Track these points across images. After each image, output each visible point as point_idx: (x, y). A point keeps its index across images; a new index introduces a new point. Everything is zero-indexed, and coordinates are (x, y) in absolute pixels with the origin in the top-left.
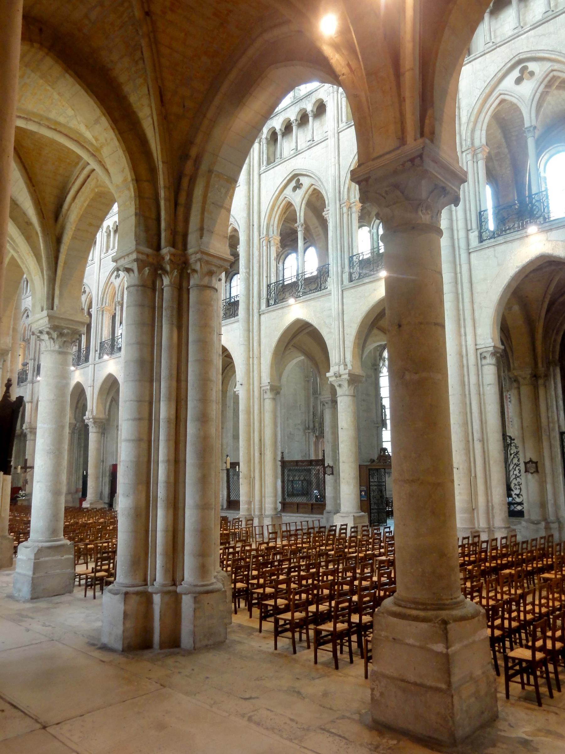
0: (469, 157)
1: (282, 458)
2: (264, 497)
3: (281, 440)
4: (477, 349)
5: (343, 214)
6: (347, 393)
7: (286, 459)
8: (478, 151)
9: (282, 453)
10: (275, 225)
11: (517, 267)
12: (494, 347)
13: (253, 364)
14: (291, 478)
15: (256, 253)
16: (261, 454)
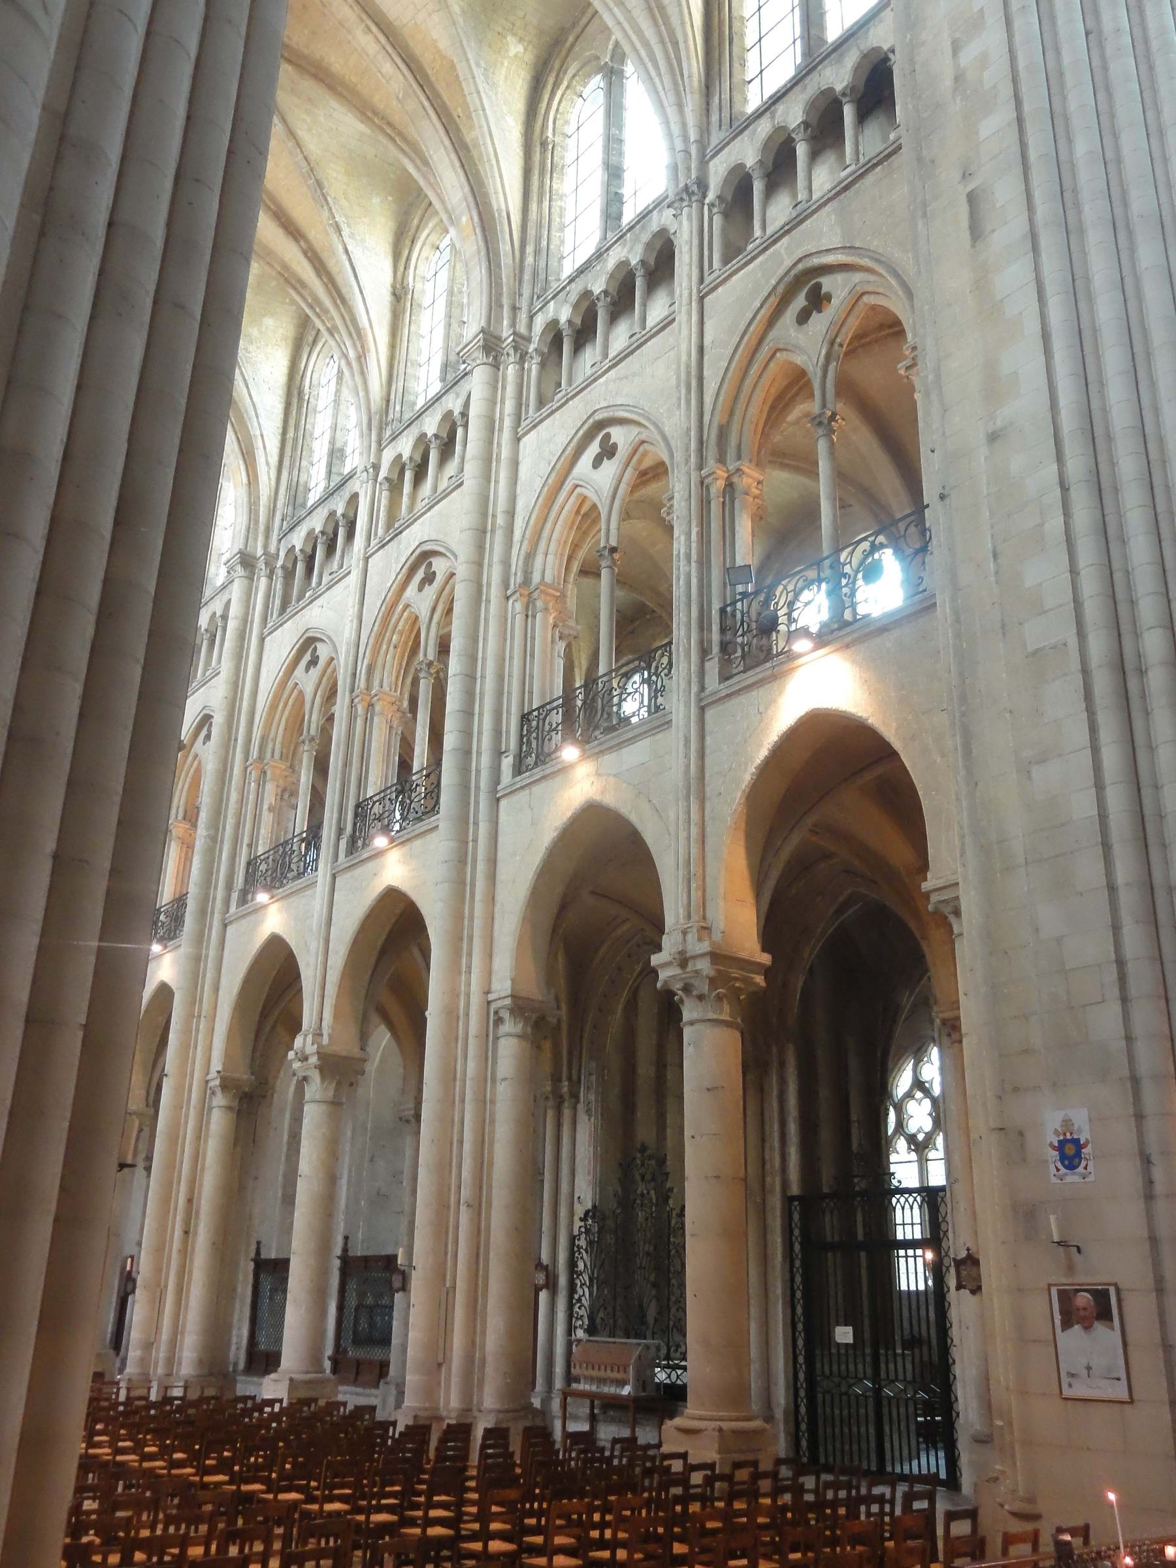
0: (519, 607)
1: (345, 1250)
2: (183, 1333)
3: (347, 1207)
4: (489, 1003)
5: (356, 718)
6: (318, 1097)
7: (351, 1254)
8: (535, 595)
9: (346, 1238)
10: (279, 739)
11: (556, 829)
12: (512, 996)
13: (197, 1030)
14: (370, 1300)
15: (234, 796)
16: (186, 1233)
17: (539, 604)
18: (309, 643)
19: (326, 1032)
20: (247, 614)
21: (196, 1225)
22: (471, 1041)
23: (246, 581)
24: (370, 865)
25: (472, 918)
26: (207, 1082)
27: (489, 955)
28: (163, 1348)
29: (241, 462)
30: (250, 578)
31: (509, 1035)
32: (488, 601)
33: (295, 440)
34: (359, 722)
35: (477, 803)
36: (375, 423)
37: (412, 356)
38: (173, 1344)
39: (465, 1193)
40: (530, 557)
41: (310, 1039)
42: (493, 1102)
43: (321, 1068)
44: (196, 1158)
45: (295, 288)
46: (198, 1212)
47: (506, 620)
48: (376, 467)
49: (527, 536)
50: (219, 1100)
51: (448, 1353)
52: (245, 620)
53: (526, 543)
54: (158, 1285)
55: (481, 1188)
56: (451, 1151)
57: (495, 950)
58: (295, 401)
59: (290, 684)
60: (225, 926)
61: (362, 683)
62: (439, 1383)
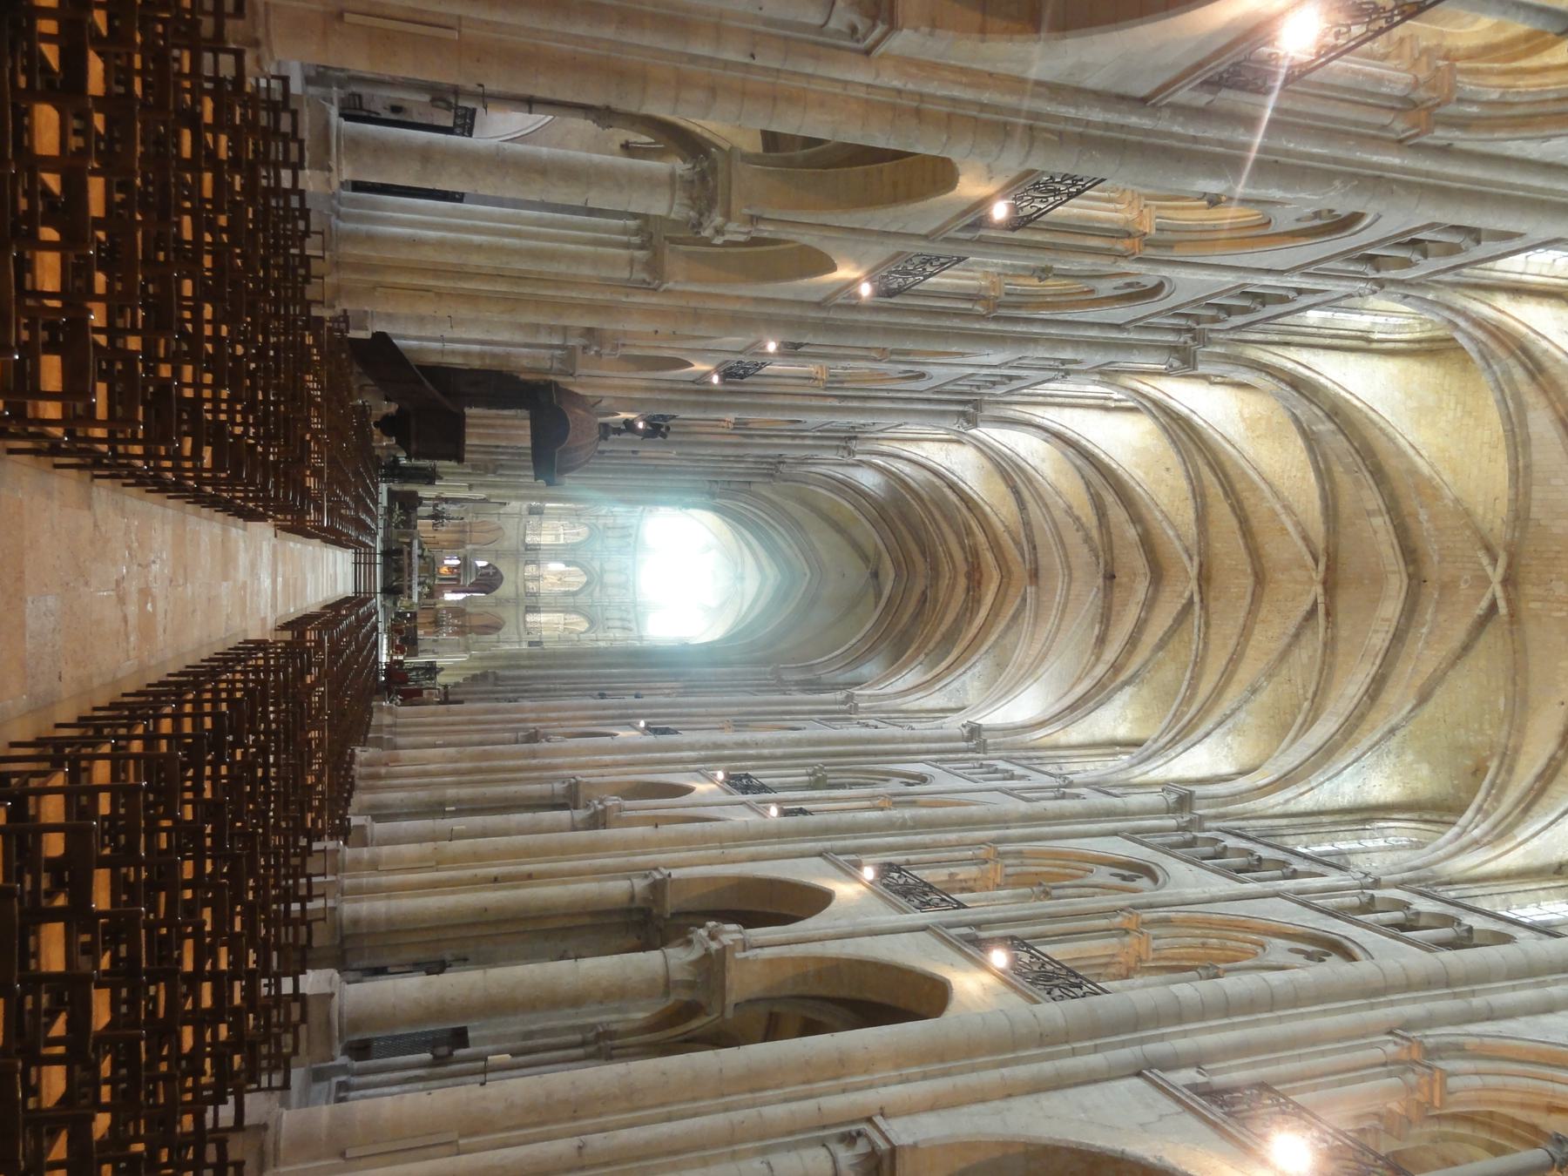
0: (1391, 1048)
2: (389, 898)
4: (869, 1120)
6: (672, 962)
8: (1418, 1069)
12: (893, 1151)
16: (496, 880)
17: (1412, 1078)
18: (1145, 870)
19: (750, 953)
20: (1134, 814)
21: (504, 888)
22: (809, 1105)
23: (1164, 806)
24: (958, 958)
25: (974, 1069)
26: (656, 869)
27: (935, 1105)
28: (372, 880)
29: (1276, 776)
30: (1169, 811)
31: (835, 1162)
32: (1372, 1007)
33: (1321, 825)
34: (1103, 923)
35: (1123, 1045)
36: (1422, 873)
37: (1513, 898)
38: (374, 891)
39: (597, 1141)
40: (1459, 1051)
41: (739, 936)
42: (734, 1156)
43: (707, 955)
44: (576, 874)
45: (1501, 764)
46: (517, 887)
47: (1363, 1037)
48: (1377, 884)
49: (1486, 1040)
50: (640, 884)
51: (363, 1162)
52: (1126, 814)
53: (1477, 1040)
54: (438, 863)
55: (607, 1164)
56: (651, 1107)
57: (944, 1113)
58: (1358, 816)
59: (1088, 866)
60: (820, 854)
61: (1147, 915)
62: (317, 1158)
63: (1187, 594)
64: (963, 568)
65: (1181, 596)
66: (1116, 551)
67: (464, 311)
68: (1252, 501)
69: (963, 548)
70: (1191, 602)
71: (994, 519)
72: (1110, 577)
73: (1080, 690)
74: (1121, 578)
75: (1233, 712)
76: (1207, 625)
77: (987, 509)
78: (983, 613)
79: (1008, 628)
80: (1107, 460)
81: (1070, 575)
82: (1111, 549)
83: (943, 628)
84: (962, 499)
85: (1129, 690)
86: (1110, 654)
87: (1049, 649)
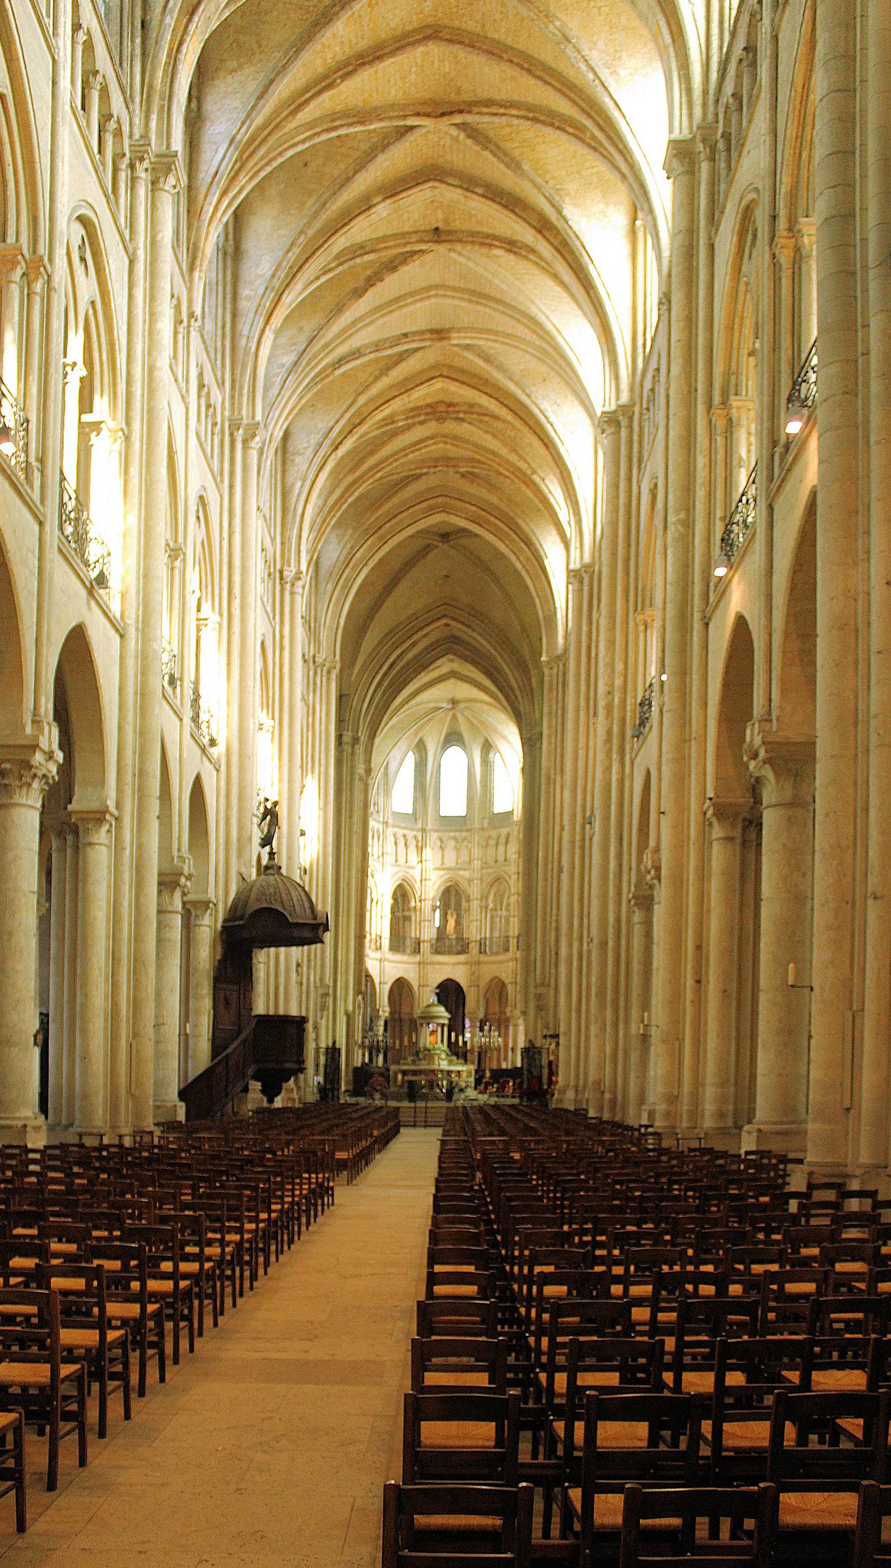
63: (454, 132)
64: (432, 427)
65: (456, 140)
66: (406, 229)
67: (149, 1011)
68: (337, 49)
69: (409, 427)
70: (462, 127)
71: (374, 391)
72: (438, 235)
73: (568, 276)
74: (437, 219)
75: (592, 69)
76: (489, 103)
77: (362, 400)
78: (484, 401)
79: (499, 367)
80: (296, 250)
81: (437, 287)
82: (403, 235)
83: (503, 451)
84: (350, 432)
85: (569, 211)
86: (527, 235)
87: (523, 313)
